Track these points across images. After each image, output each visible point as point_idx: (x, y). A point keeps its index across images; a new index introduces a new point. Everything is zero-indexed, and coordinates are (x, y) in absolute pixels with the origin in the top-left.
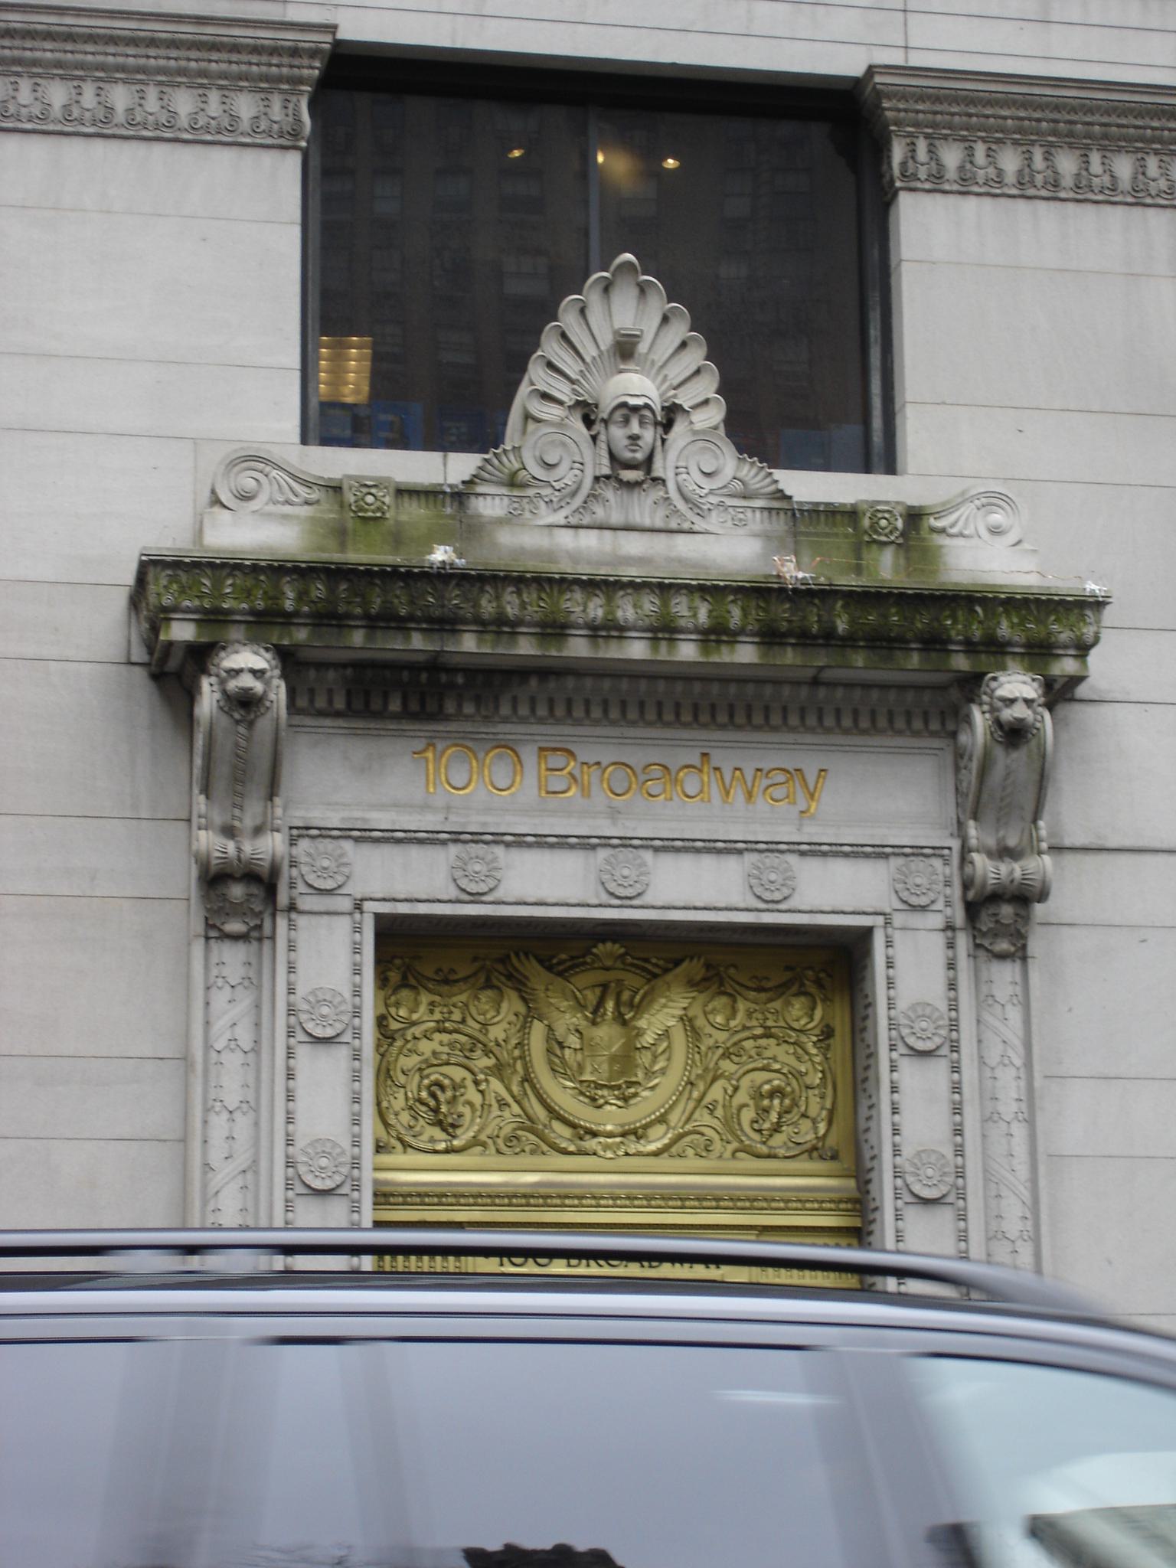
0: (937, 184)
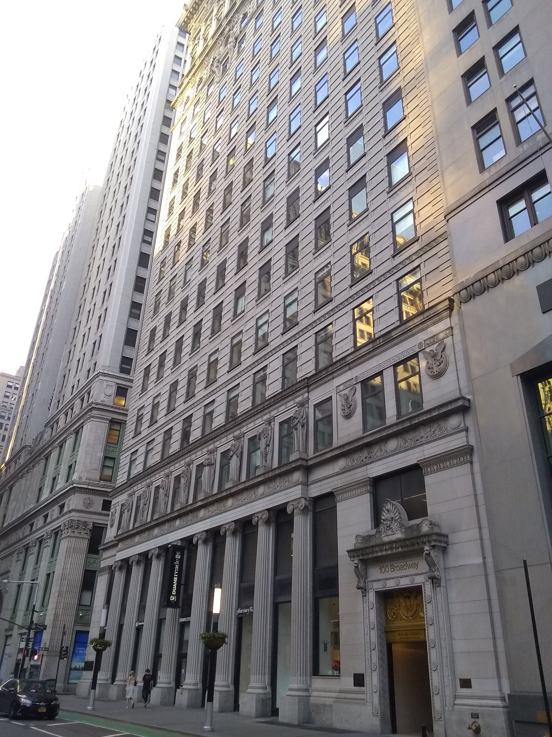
0: (428, 474)
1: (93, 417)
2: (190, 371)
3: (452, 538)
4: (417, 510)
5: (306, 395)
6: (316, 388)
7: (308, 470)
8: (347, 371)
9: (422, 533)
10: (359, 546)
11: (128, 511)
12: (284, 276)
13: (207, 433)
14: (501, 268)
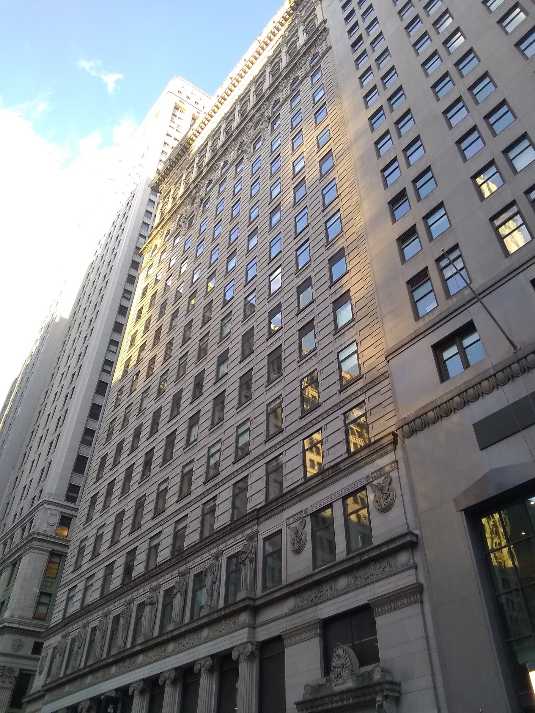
1: (33, 548)
2: (137, 500)
3: (405, 687)
4: (368, 654)
5: (255, 528)
6: (267, 519)
7: (255, 609)
8: (297, 503)
9: (374, 682)
10: (308, 697)
11: (60, 655)
12: (237, 406)
13: (150, 569)
14: (439, 406)
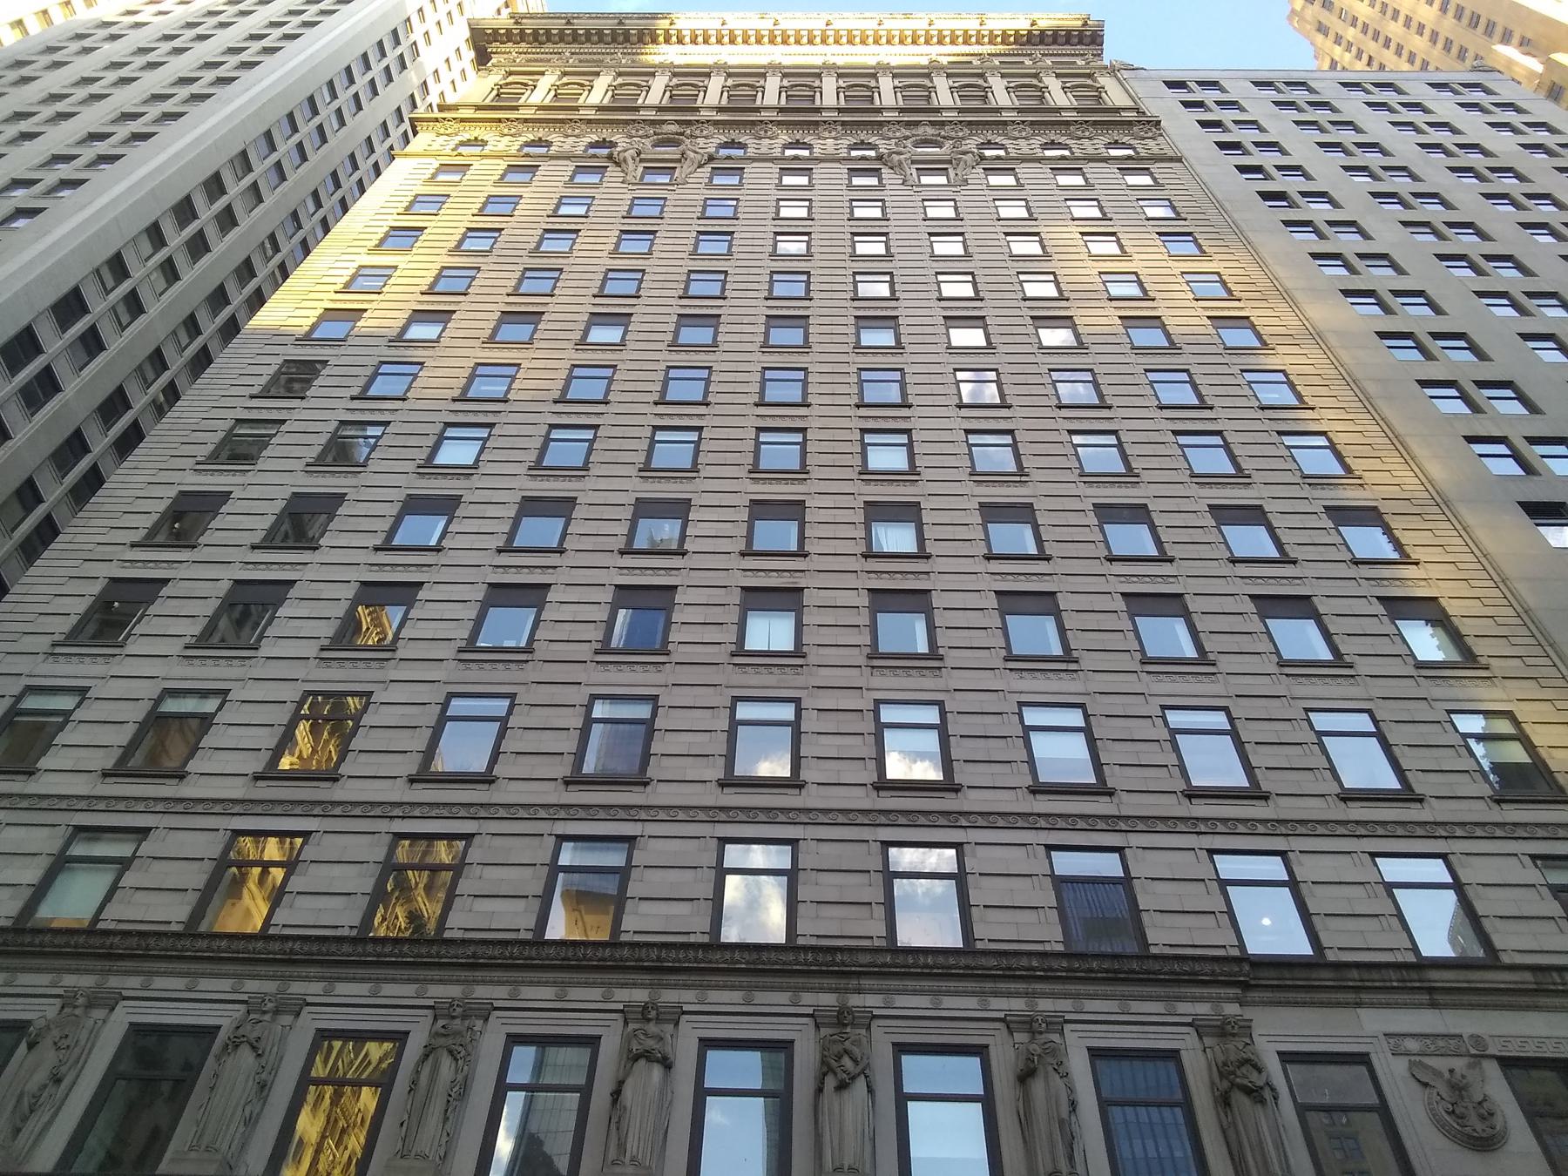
5: (1231, 1009)
8: (1420, 1006)
